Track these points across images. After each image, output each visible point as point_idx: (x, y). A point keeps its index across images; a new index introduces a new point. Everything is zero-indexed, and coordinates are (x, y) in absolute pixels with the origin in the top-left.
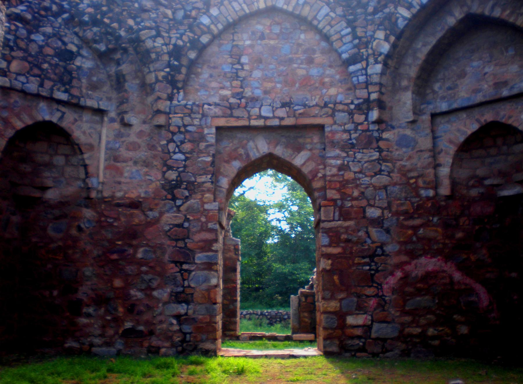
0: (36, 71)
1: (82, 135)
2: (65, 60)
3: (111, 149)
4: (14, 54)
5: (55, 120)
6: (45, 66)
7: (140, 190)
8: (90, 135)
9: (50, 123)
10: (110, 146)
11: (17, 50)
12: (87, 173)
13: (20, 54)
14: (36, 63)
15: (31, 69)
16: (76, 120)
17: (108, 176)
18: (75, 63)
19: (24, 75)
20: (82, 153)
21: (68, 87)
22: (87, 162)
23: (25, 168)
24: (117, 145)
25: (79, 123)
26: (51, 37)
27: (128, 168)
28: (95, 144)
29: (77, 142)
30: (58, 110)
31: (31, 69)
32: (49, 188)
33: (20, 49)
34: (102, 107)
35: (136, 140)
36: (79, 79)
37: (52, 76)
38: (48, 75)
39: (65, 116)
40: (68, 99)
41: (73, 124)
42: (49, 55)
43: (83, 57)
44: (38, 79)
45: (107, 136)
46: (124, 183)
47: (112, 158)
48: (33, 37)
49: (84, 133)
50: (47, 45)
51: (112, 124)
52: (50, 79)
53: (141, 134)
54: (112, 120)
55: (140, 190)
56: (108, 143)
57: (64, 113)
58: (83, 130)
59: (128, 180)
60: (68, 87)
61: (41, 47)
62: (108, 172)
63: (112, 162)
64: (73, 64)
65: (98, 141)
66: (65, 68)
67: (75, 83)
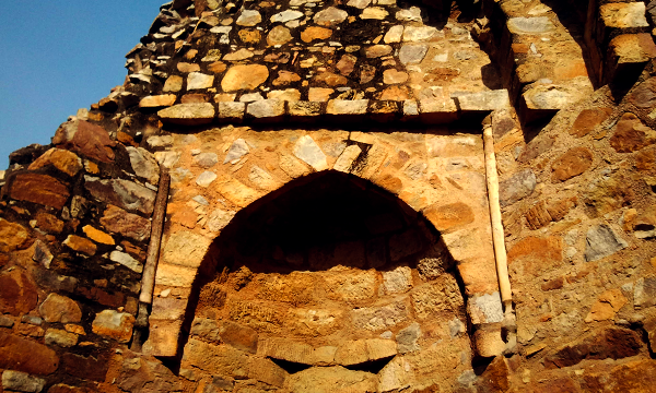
0: (285, 76)
1: (428, 187)
2: (359, 40)
3: (517, 198)
4: (228, 57)
5: (343, 166)
6: (308, 63)
7: (628, 285)
8: (453, 183)
9: (330, 175)
10: (511, 190)
11: (238, 49)
12: (462, 285)
13: (245, 53)
14: (285, 61)
15: (273, 75)
16: (403, 156)
17: (520, 277)
18: (385, 40)
19: (258, 89)
20: (438, 235)
21: (372, 89)
22: (456, 254)
23: (316, 318)
24: (529, 182)
25: (414, 161)
26: (321, 9)
27: (573, 231)
28: (475, 203)
29: (416, 207)
30: (350, 142)
31: (273, 75)
32: (384, 362)
33: (247, 45)
34: (467, 106)
35: (574, 142)
36: (401, 68)
37: (329, 77)
38: (318, 78)
39: (371, 152)
40: (369, 109)
41: (398, 166)
42: (318, 41)
43: (403, 23)
44: (292, 90)
45: (499, 172)
46: (571, 280)
47: (523, 220)
48: (275, 18)
49: (434, 181)
50: (311, 23)
51: (505, 136)
52: (323, 84)
53: (583, 123)
54: (504, 127)
55: (628, 285)
56: (503, 185)
57: (365, 147)
58: (429, 176)
59: (581, 266)
60: (372, 89)
61: (296, 33)
62: (519, 264)
63: (526, 232)
64: (382, 42)
65: (481, 192)
66: (359, 55)
67: (390, 77)
